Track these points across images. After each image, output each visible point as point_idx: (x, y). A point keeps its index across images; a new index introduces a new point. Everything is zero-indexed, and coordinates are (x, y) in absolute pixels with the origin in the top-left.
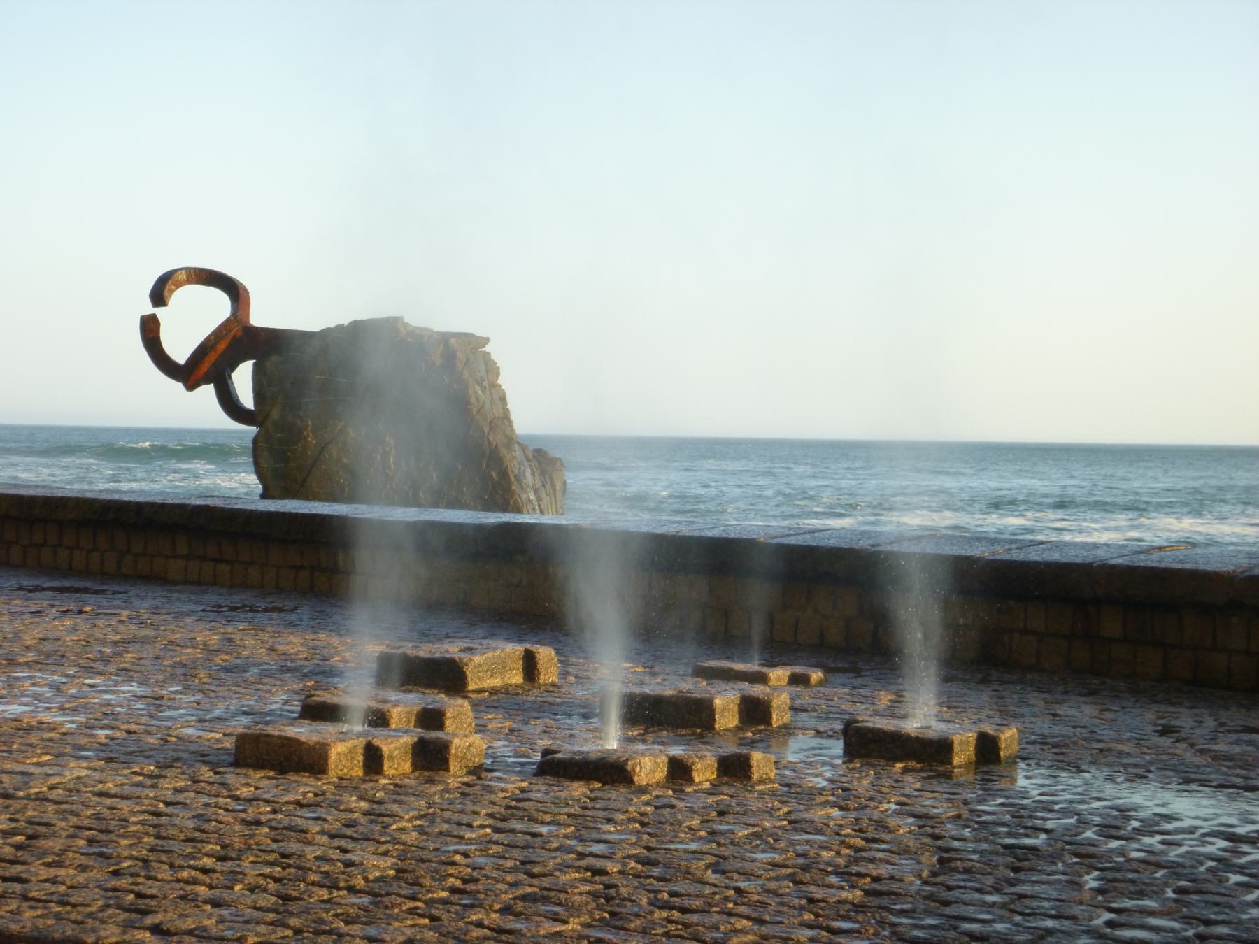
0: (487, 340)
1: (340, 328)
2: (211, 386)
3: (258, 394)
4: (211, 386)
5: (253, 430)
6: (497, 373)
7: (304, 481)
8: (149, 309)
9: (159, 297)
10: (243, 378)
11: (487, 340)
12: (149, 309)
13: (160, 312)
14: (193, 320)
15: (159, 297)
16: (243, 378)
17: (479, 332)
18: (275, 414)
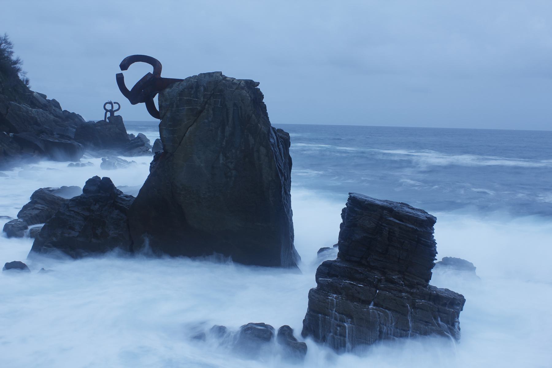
0: (259, 83)
1: (195, 77)
2: (144, 104)
3: (160, 107)
4: (144, 104)
5: (159, 121)
6: (262, 96)
7: (180, 143)
8: (120, 71)
9: (125, 65)
10: (156, 100)
11: (259, 83)
12: (120, 71)
13: (124, 72)
14: (135, 74)
15: (125, 65)
16: (156, 100)
17: (255, 80)
18: (168, 115)
